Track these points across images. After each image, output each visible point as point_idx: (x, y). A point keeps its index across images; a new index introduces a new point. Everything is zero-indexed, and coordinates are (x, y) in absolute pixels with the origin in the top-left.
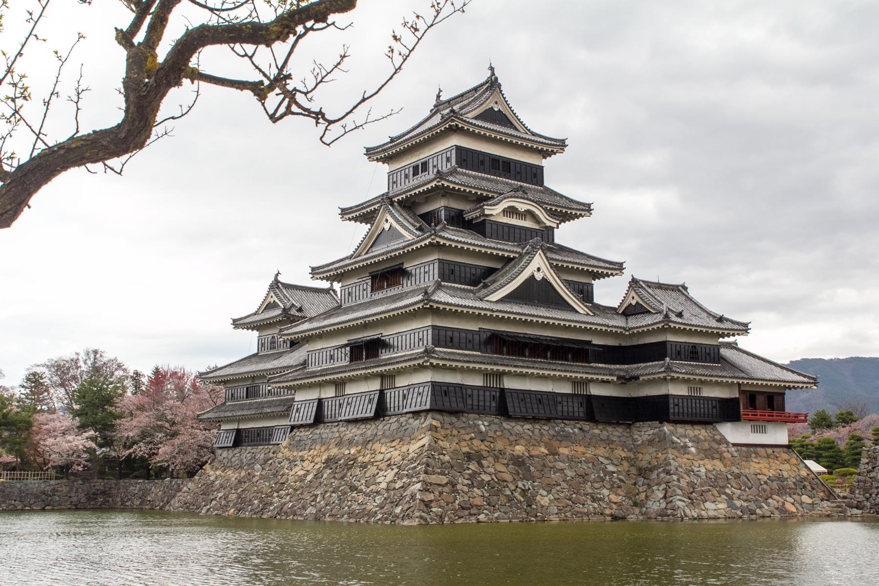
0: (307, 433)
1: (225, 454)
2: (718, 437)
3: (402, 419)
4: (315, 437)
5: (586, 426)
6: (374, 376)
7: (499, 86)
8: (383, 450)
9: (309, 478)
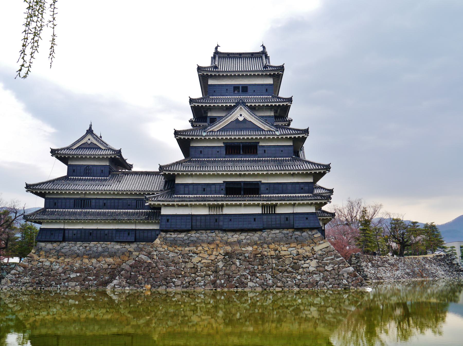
0: (180, 236)
1: (49, 246)
3: (285, 231)
4: (195, 239)
6: (258, 205)
8: (283, 248)
9: (221, 264)
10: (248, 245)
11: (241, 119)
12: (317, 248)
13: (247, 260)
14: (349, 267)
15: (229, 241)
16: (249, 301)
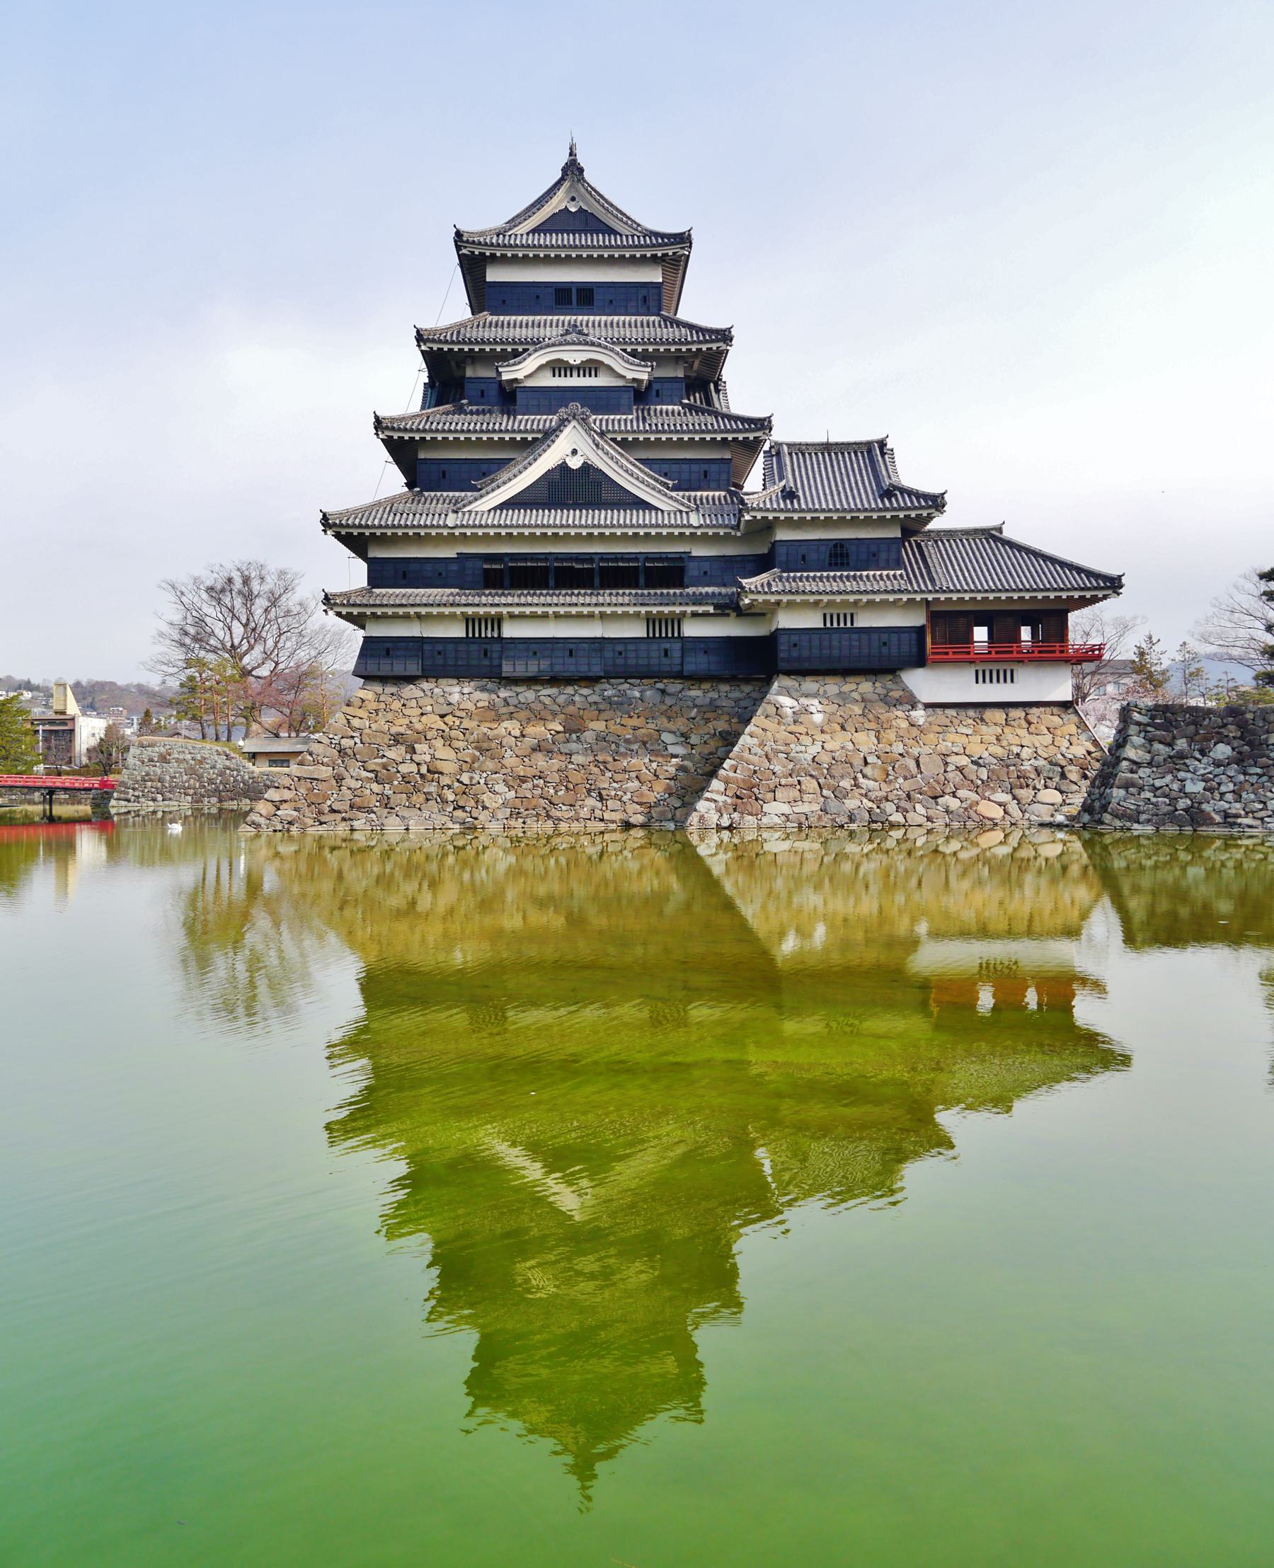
2: (896, 694)
5: (674, 687)
7: (581, 170)
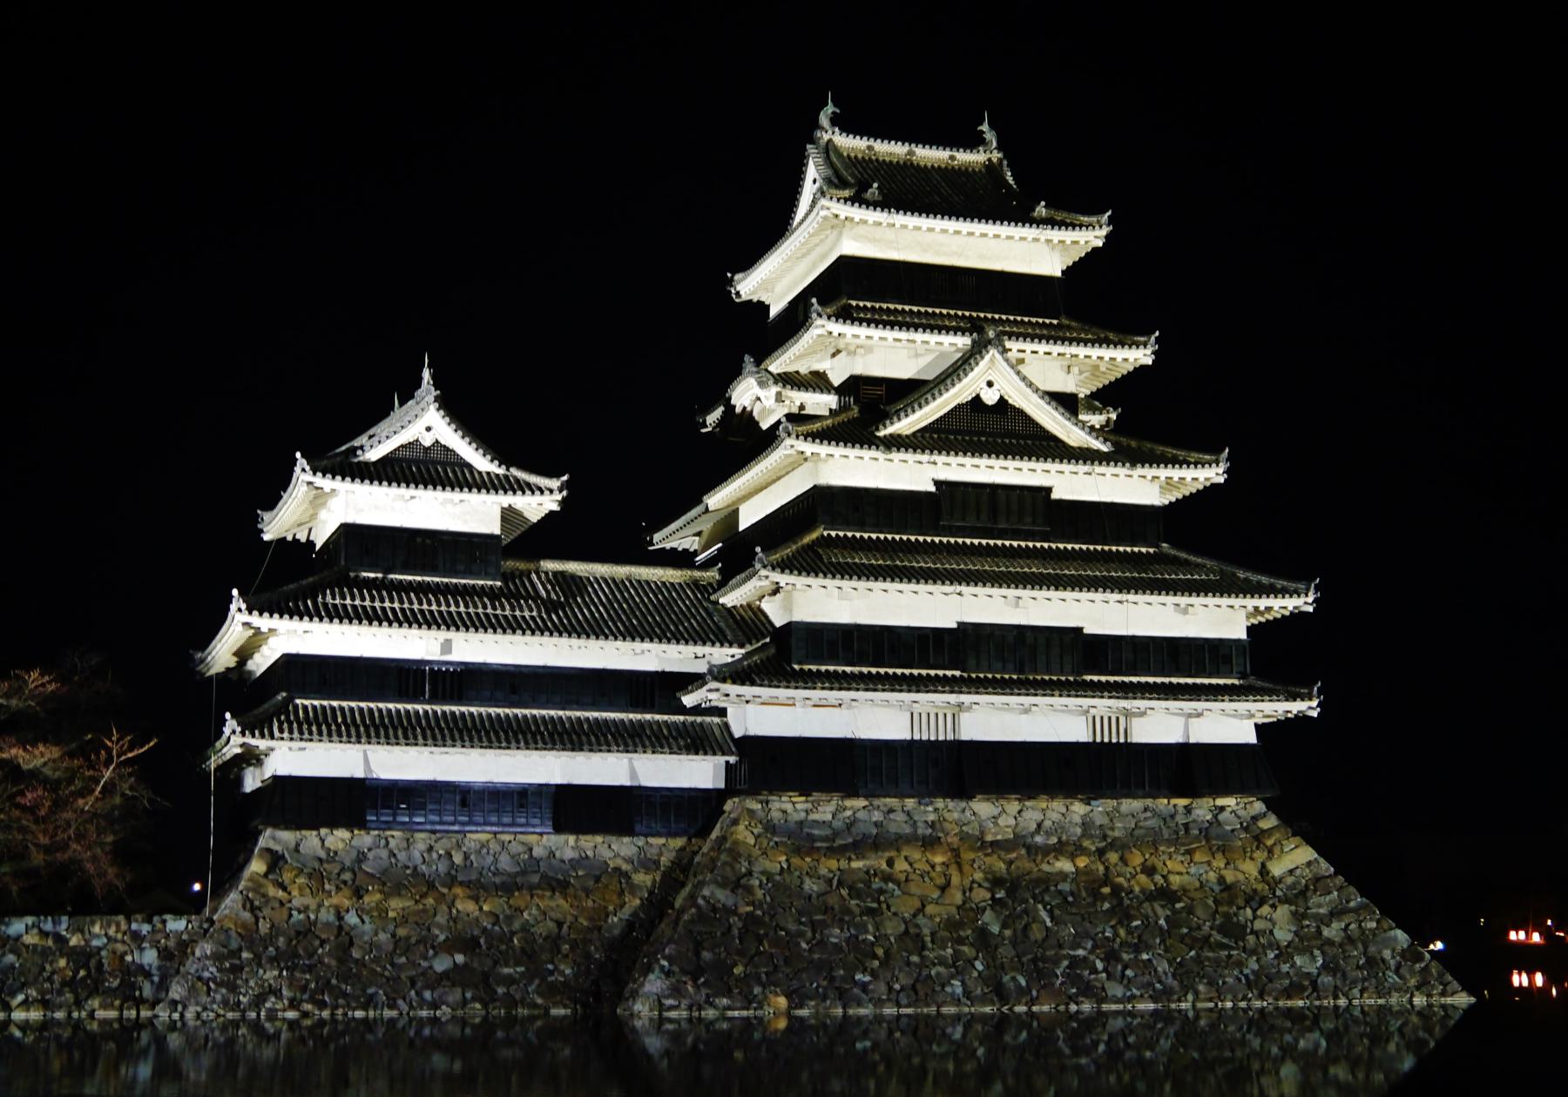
10: (1060, 849)
11: (990, 398)
12: (1277, 869)
13: (1064, 906)
14: (1391, 929)
15: (989, 838)
16: (1102, 1048)
